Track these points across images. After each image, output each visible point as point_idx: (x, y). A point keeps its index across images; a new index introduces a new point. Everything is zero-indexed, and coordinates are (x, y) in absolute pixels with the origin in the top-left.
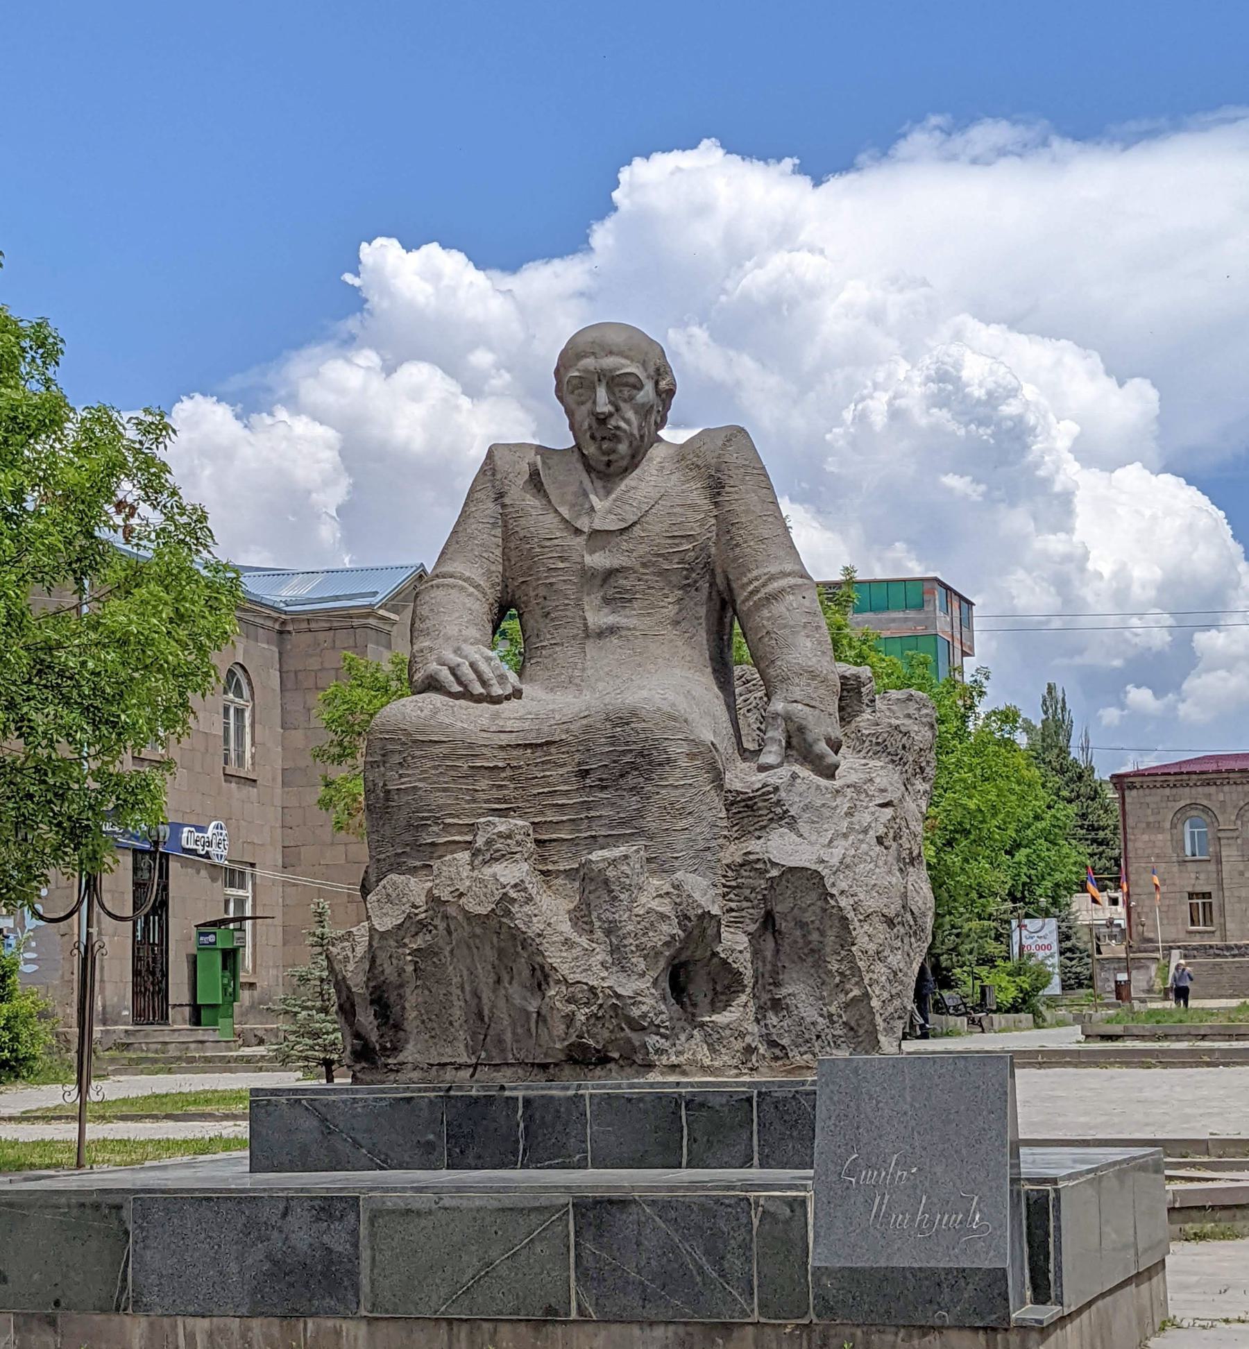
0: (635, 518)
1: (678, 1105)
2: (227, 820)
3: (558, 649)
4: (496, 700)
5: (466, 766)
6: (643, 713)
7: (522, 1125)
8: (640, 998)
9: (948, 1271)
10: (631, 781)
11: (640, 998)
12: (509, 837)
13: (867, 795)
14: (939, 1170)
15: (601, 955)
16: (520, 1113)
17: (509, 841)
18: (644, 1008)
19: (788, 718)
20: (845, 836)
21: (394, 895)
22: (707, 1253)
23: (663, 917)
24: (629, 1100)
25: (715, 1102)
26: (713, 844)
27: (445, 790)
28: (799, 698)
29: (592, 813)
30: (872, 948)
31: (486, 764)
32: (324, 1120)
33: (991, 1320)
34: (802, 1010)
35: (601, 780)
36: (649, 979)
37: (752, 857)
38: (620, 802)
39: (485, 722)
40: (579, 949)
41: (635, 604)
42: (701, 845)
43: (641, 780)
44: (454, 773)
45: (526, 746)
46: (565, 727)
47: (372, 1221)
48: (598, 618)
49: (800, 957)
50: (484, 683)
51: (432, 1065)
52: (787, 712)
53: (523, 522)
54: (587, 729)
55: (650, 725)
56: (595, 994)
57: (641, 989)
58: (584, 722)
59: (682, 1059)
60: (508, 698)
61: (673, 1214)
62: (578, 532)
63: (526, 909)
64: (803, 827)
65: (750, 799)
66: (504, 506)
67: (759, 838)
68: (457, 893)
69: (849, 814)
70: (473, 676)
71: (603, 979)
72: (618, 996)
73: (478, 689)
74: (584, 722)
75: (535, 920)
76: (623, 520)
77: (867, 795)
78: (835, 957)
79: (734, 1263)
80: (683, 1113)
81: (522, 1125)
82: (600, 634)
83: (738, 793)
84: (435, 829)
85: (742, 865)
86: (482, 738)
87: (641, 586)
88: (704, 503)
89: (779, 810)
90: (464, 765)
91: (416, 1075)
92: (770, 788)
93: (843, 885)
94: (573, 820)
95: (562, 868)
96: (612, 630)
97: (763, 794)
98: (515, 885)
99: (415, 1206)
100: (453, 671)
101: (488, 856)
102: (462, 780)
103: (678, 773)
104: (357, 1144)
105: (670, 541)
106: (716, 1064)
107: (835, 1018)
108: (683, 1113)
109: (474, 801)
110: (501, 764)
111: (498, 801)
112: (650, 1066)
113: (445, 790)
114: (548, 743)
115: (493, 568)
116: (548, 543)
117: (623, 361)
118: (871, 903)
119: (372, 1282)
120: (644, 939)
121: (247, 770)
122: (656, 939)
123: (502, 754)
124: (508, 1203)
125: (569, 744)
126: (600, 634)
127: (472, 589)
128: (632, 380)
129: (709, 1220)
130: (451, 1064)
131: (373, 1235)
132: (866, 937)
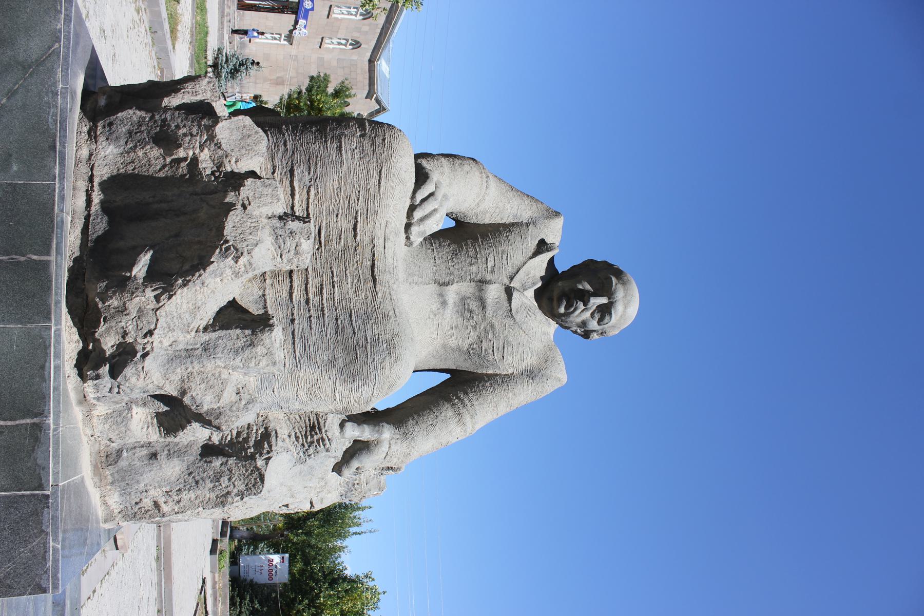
0: (517, 320)
1: (37, 415)
2: (308, 37)
3: (432, 261)
4: (408, 227)
5: (359, 208)
6: (396, 367)
7: (22, 259)
8: (142, 375)
11: (142, 375)
12: (297, 253)
13: (319, 492)
16: (35, 257)
17: (292, 252)
18: (133, 380)
19: (377, 443)
21: (249, 141)
23: (219, 397)
24: (43, 367)
25: (39, 454)
27: (339, 189)
28: (393, 448)
29: (314, 321)
31: (359, 226)
34: (148, 475)
35: (343, 331)
37: (273, 439)
38: (323, 346)
39: (392, 225)
40: (190, 320)
41: (460, 319)
43: (341, 365)
44: (353, 197)
45: (373, 260)
46: (388, 295)
48: (452, 293)
49: (191, 473)
50: (422, 220)
51: (92, 169)
52: (382, 441)
53: (518, 238)
54: (385, 316)
55: (387, 371)
56: (145, 336)
58: (391, 314)
60: (408, 238)
62: (512, 278)
63: (229, 272)
64: (299, 467)
65: (320, 429)
66: (528, 224)
67: (289, 436)
68: (247, 203)
70: (427, 212)
71: (161, 342)
72: (145, 356)
73: (418, 214)
74: (391, 314)
75: (219, 279)
76: (517, 312)
77: (319, 492)
78: (193, 497)
80: (28, 421)
81: (22, 259)
82: (441, 295)
83: (325, 420)
84: (307, 178)
85: (266, 428)
86: (380, 220)
87: (472, 323)
88: (523, 366)
89: (311, 451)
91: (84, 153)
92: (328, 445)
94: (307, 301)
95: (267, 292)
96: (444, 303)
97: (323, 440)
98: (250, 264)
100: (432, 194)
101: (279, 232)
102: (347, 204)
105: (501, 344)
106: (95, 420)
107: (144, 494)
108: (28, 421)
109: (329, 213)
110: (358, 238)
111: (328, 236)
112: (82, 376)
113: (339, 189)
114: (374, 280)
115: (488, 215)
116: (504, 257)
120: (198, 379)
121: (324, 46)
123: (367, 239)
125: (374, 300)
126: (441, 295)
127: (477, 201)
128: (606, 321)
130: (92, 186)
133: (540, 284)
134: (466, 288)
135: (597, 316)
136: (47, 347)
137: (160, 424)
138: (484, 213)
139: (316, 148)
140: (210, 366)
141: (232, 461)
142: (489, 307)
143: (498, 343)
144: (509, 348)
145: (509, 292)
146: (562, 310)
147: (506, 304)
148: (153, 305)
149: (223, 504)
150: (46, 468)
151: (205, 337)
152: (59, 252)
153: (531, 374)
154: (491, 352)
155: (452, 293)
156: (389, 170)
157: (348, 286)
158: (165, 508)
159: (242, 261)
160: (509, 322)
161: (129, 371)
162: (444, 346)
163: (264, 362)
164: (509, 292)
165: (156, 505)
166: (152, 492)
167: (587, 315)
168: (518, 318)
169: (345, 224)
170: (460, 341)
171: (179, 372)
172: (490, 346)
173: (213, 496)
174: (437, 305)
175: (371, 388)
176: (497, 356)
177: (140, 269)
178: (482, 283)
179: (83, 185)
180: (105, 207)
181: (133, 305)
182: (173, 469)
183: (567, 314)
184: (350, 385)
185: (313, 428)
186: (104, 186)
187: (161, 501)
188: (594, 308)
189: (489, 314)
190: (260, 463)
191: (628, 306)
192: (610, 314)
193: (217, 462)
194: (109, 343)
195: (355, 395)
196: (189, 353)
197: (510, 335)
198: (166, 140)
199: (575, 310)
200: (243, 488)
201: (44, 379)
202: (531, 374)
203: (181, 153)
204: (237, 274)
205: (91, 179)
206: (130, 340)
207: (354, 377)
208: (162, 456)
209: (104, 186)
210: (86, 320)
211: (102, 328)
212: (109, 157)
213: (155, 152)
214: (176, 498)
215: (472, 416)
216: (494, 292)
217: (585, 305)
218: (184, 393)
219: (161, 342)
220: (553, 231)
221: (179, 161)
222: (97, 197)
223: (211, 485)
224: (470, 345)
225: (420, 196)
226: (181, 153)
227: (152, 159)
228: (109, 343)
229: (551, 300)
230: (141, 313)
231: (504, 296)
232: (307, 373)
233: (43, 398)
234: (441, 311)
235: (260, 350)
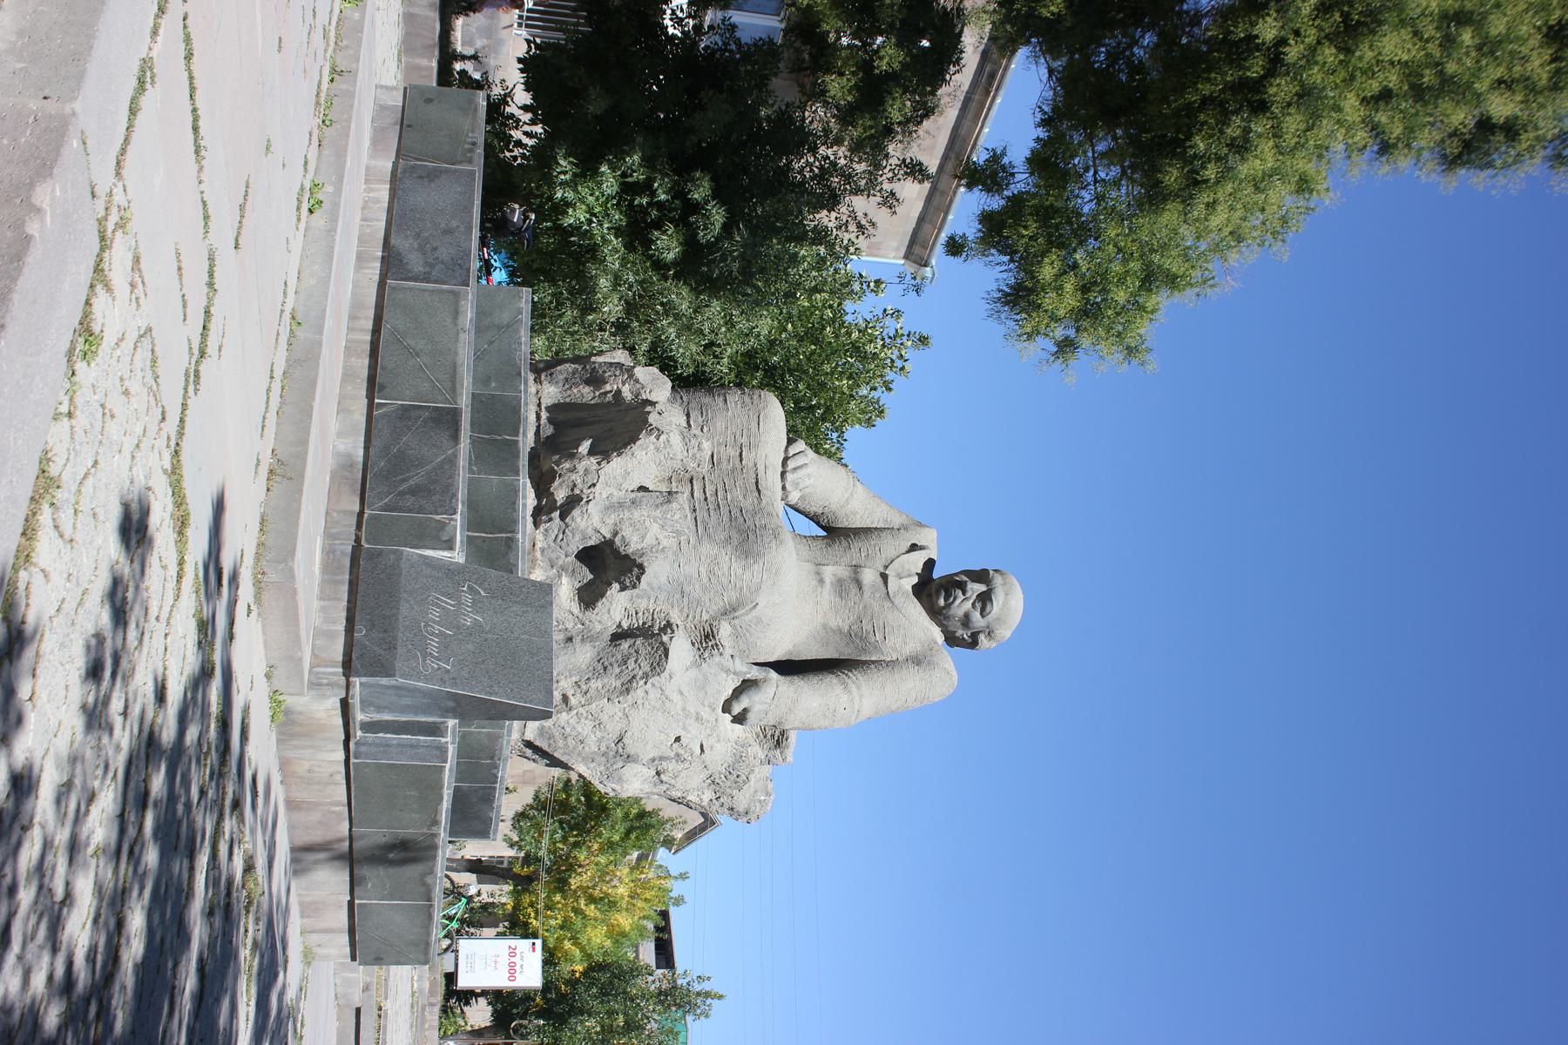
4: (783, 474)
9: (395, 638)
10: (735, 535)
14: (470, 647)
15: (618, 495)
20: (684, 709)
22: (417, 485)
23: (643, 538)
30: (605, 718)
32: (508, 326)
33: (356, 663)
36: (598, 525)
42: (687, 589)
47: (452, 292)
48: (829, 572)
57: (591, 524)
59: (538, 554)
61: (446, 467)
69: (698, 718)
73: (791, 464)
79: (410, 501)
82: (818, 573)
86: (762, 452)
88: (910, 648)
90: (744, 440)
93: (651, 695)
96: (821, 581)
99: (461, 318)
103: (740, 571)
104: (491, 343)
112: (536, 525)
118: (637, 718)
119: (410, 289)
122: (626, 532)
123: (751, 464)
124: (459, 370)
126: (818, 573)
128: (988, 608)
129: (436, 491)
131: (442, 291)
132: (612, 712)
133: (915, 580)
134: (843, 571)
135: (978, 605)
136: (516, 491)
137: (581, 600)
138: (854, 514)
139: (707, 400)
140: (637, 514)
141: (639, 641)
142: (865, 588)
143: (879, 623)
145: (884, 577)
146: (942, 602)
148: (596, 467)
149: (628, 691)
150: (516, 566)
151: (633, 495)
152: (525, 435)
153: (917, 660)
155: (829, 572)
156: (766, 417)
157: (738, 493)
158: (573, 701)
159: (663, 438)
160: (887, 604)
161: (576, 512)
162: (825, 627)
163: (677, 517)
164: (884, 577)
165: (565, 699)
166: (562, 683)
167: (968, 605)
168: (897, 601)
169: (734, 453)
170: (841, 621)
171: (612, 519)
173: (618, 684)
174: (814, 583)
176: (879, 637)
177: (584, 447)
178: (856, 568)
179: (533, 408)
180: (550, 420)
181: (581, 467)
182: (584, 655)
183: (948, 606)
185: (707, 637)
186: (548, 409)
187: (569, 694)
189: (867, 595)
190: (665, 638)
191: (1010, 604)
193: (625, 645)
194: (560, 495)
195: (748, 574)
196: (621, 505)
198: (595, 380)
200: (647, 669)
201: (515, 510)
202: (917, 660)
203: (608, 387)
204: (657, 449)
205: (539, 405)
206: (577, 491)
207: (746, 554)
208: (577, 640)
209: (548, 409)
210: (542, 484)
211: (556, 483)
212: (551, 393)
213: (586, 390)
214: (584, 687)
215: (859, 688)
216: (869, 576)
218: (616, 534)
219: (601, 493)
220: (928, 537)
221: (606, 393)
222: (544, 415)
223: (617, 671)
225: (791, 452)
226: (608, 387)
227: (586, 393)
228: (560, 495)
229: (930, 595)
230: (587, 471)
231: (879, 579)
232: (708, 549)
233: (515, 522)
235: (675, 505)
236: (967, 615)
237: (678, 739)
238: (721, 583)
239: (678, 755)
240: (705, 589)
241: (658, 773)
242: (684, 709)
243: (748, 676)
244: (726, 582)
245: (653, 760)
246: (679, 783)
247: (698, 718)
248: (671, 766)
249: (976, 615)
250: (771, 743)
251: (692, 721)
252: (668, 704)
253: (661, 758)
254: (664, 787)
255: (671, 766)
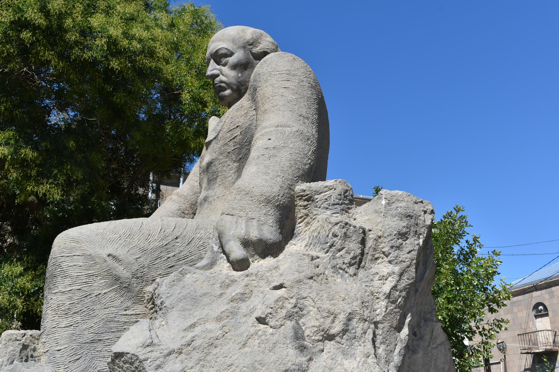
26: (105, 336)
41: (219, 180)
42: (88, 336)
69: (243, 297)
103: (68, 281)
105: (229, 134)
117: (218, 43)
135: (224, 60)
144: (231, 125)
147: (213, 143)
154: (235, 140)
160: (220, 135)
167: (226, 69)
172: (231, 143)
175: (67, 259)
183: (229, 86)
184: (59, 279)
188: (218, 67)
189: (214, 156)
192: (217, 51)
195: (74, 272)
197: (226, 129)
199: (222, 82)
217: (217, 76)
224: (234, 162)
234: (210, 200)
236: (234, 67)
237: (261, 320)
238: (80, 300)
239: (289, 317)
240: (90, 316)
241: (331, 338)
242: (219, 319)
243: (216, 248)
244: (79, 294)
245: (302, 348)
246: (343, 309)
247: (243, 297)
248: (310, 323)
249: (232, 60)
250: (311, 207)
251: (244, 307)
252: (197, 343)
253: (298, 336)
254: (358, 326)
255: (310, 323)
